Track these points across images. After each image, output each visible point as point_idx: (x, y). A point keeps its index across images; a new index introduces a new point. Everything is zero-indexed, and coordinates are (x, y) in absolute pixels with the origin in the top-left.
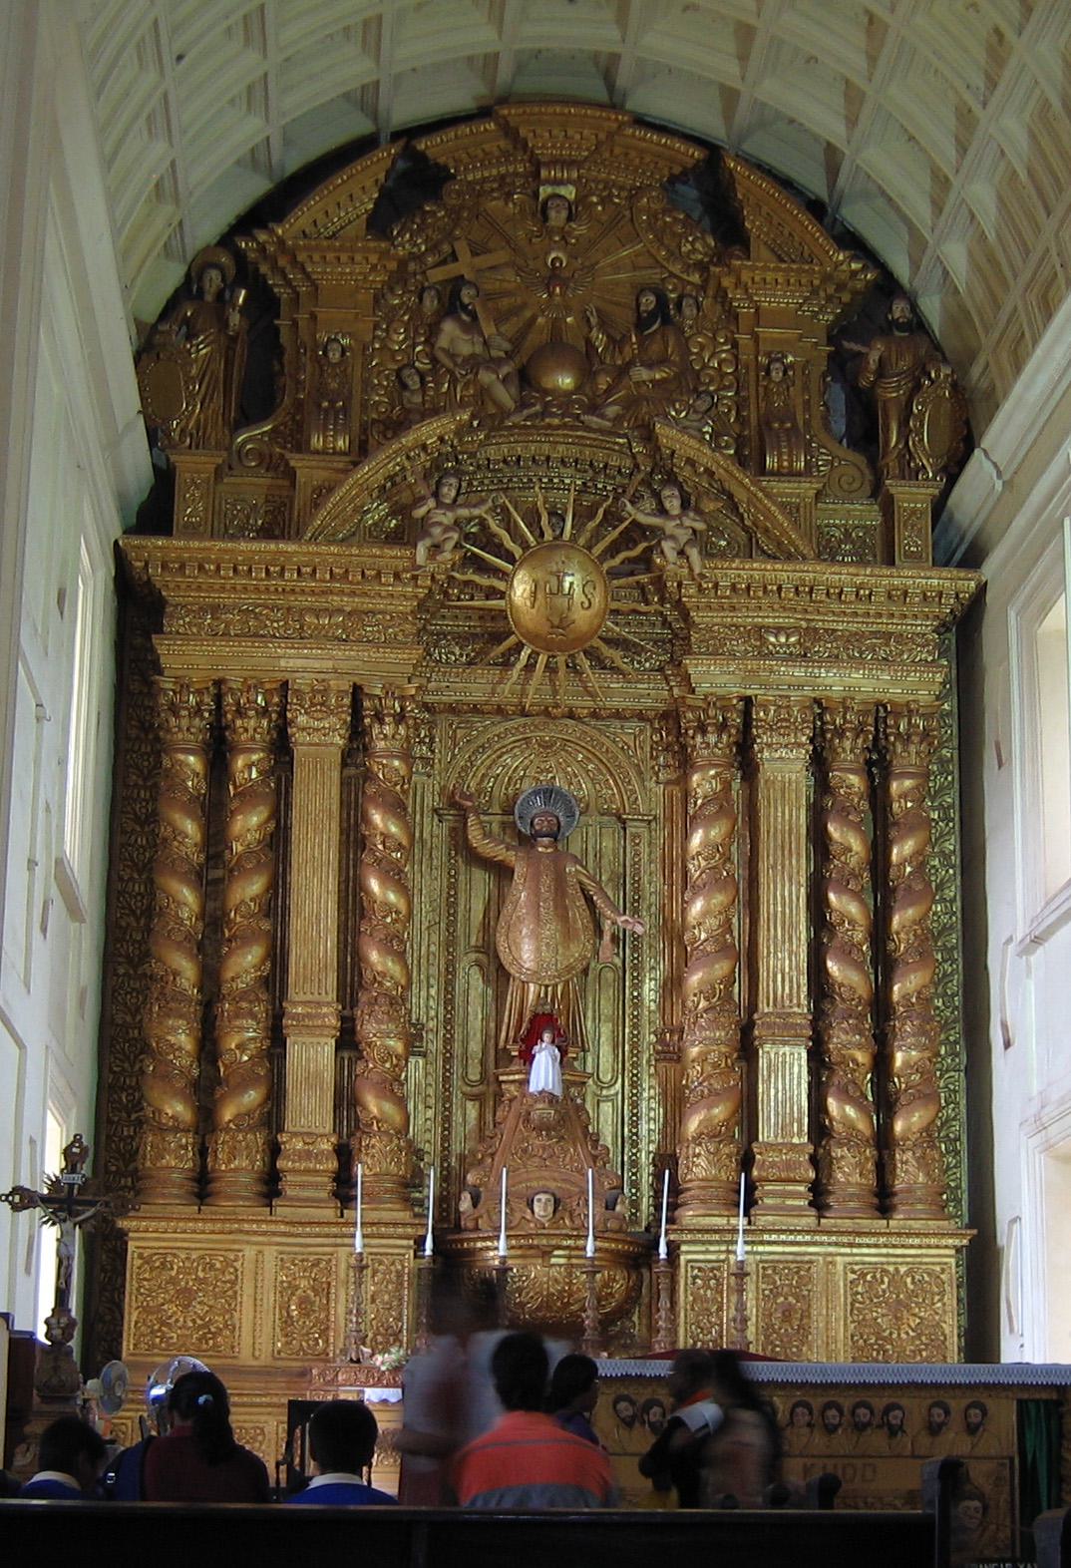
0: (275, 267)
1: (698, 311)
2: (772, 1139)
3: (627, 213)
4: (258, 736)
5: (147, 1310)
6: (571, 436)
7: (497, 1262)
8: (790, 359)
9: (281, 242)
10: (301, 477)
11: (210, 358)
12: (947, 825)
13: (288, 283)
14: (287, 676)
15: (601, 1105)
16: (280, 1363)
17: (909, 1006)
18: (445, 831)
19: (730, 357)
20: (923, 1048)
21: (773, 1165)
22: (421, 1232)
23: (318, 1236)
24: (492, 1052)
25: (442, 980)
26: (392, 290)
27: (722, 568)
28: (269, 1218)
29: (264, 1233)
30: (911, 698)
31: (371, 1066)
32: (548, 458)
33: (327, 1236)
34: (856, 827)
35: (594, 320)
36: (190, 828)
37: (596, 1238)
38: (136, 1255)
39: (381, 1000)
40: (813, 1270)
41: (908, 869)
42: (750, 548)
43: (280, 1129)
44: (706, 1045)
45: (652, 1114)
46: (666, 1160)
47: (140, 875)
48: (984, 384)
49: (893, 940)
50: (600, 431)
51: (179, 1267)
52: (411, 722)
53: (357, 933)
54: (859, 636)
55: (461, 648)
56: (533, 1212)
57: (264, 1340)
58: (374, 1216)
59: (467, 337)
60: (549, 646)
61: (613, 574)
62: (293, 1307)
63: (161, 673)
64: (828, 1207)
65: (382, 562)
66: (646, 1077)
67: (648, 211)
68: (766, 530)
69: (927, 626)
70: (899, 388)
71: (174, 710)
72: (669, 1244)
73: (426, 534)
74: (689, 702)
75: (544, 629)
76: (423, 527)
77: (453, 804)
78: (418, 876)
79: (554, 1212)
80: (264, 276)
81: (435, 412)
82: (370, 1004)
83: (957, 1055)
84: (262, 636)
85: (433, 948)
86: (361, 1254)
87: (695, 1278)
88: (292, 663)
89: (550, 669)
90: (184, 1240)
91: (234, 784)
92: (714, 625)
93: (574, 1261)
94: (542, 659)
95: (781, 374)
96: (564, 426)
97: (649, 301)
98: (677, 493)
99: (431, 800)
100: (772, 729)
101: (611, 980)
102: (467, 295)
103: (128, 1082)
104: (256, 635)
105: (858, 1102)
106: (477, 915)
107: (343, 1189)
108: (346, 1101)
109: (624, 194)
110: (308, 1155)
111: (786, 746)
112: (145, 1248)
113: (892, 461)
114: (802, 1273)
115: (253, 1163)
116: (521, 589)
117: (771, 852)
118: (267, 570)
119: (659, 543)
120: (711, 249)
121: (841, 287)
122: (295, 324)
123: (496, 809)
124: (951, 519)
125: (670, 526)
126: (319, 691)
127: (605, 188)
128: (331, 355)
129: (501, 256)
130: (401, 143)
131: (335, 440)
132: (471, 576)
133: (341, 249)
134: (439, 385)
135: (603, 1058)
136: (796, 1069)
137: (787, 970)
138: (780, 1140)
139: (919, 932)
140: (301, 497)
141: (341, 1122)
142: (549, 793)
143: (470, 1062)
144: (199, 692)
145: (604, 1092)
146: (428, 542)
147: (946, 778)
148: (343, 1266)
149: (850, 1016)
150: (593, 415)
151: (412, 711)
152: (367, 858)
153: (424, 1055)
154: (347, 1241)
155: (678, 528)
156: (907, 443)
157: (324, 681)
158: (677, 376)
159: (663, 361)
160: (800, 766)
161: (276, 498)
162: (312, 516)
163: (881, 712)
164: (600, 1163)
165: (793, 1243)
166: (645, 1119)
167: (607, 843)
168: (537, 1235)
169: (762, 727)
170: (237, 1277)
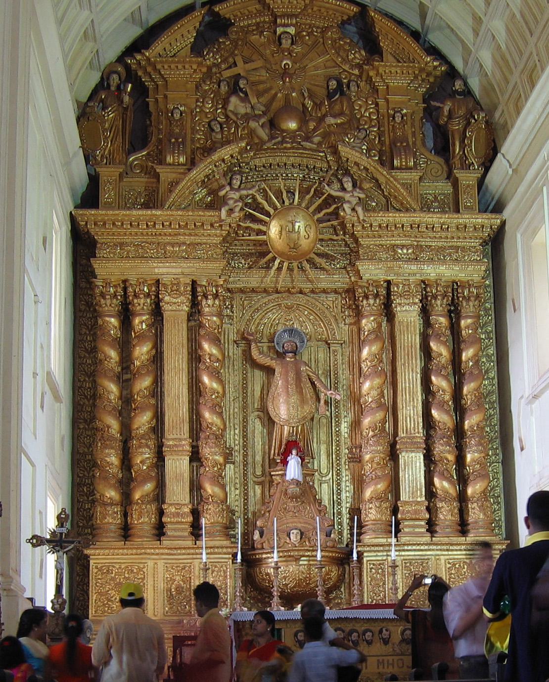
0: (146, 72)
1: (358, 88)
2: (407, 499)
3: (321, 40)
4: (145, 307)
5: (100, 594)
6: (297, 153)
7: (273, 564)
8: (405, 111)
9: (148, 59)
10: (162, 177)
11: (115, 118)
12: (489, 341)
13: (152, 80)
14: (159, 277)
15: (322, 485)
16: (167, 618)
17: (473, 431)
18: (240, 352)
19: (374, 111)
20: (481, 452)
21: (408, 512)
22: (235, 551)
23: (184, 554)
24: (267, 460)
25: (241, 426)
26: (204, 82)
27: (374, 217)
28: (159, 546)
29: (157, 554)
30: (470, 278)
31: (207, 469)
32: (285, 164)
33: (189, 554)
34: (444, 343)
35: (306, 95)
36: (113, 354)
37: (322, 551)
38: (94, 567)
39: (211, 437)
40: (430, 563)
41: (471, 364)
42: (387, 207)
43: (163, 502)
44: (373, 453)
45: (347, 489)
46: (355, 511)
47: (89, 379)
48: (502, 121)
49: (464, 399)
50: (310, 149)
51: (116, 572)
52: (221, 298)
53: (198, 403)
54: (443, 248)
55: (245, 260)
56: (290, 539)
57: (159, 605)
58: (211, 544)
59: (243, 105)
60: (289, 258)
61: (320, 221)
62: (173, 590)
63: (96, 278)
64: (436, 532)
65: (204, 219)
66: (344, 470)
67: (331, 39)
68: (395, 197)
69: (476, 242)
70: (459, 124)
71: (103, 295)
72: (358, 552)
73: (226, 204)
74: (359, 284)
75: (286, 250)
76: (224, 201)
77: (244, 338)
78: (227, 375)
80: (140, 76)
81: (229, 142)
82: (205, 439)
83: (498, 455)
84: (147, 257)
85: (236, 410)
86: (206, 562)
87: (371, 569)
88: (161, 270)
89: (290, 269)
90: (118, 559)
91: (134, 331)
92: (370, 245)
93: (311, 563)
94: (286, 264)
95: (400, 119)
96: (293, 148)
97: (333, 84)
98: (350, 180)
99: (233, 336)
100: (401, 296)
101: (325, 423)
102: (242, 84)
103: (87, 481)
104: (143, 257)
105: (449, 479)
106: (258, 393)
107: (196, 530)
108: (196, 487)
109: (319, 30)
110: (178, 514)
111: (408, 304)
112: (99, 563)
113: (457, 161)
114: (424, 565)
115: (150, 519)
116: (274, 230)
117: (403, 357)
118: (147, 224)
119: (342, 204)
120: (363, 56)
121: (428, 75)
122: (157, 100)
123: (265, 340)
124: (487, 188)
125: (347, 196)
126: (175, 284)
127: (310, 27)
128: (175, 115)
129: (259, 63)
130: (207, 7)
131: (179, 158)
132: (249, 224)
133: (178, 62)
134: (229, 129)
135: (322, 462)
136: (418, 464)
137: (412, 415)
138: (411, 500)
139: (477, 395)
140: (163, 187)
141: (194, 498)
142: (291, 331)
143: (256, 466)
144: (115, 286)
145: (324, 479)
146: (227, 208)
147: (488, 318)
148: (197, 568)
149: (444, 437)
150: (307, 141)
151: (222, 292)
152: (202, 366)
153: (234, 463)
154: (198, 556)
155: (351, 197)
156: (464, 151)
157: (177, 278)
158: (349, 122)
159: (341, 114)
160: (415, 314)
161: (150, 188)
162: (169, 197)
163: (455, 287)
164: (323, 514)
165: (419, 550)
166: (344, 491)
167: (321, 355)
168: (293, 550)
169: (396, 295)
170: (145, 576)
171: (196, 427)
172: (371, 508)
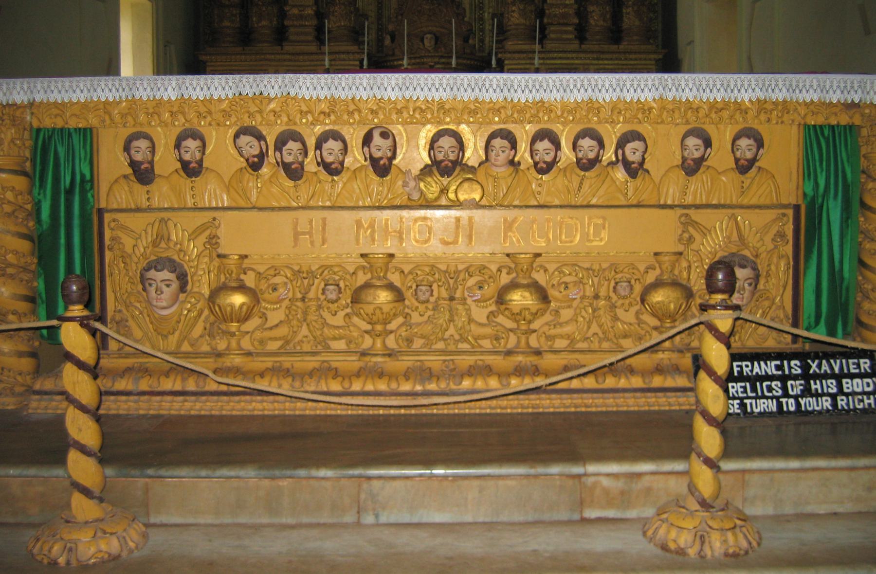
37: (457, 58)
79: (436, 43)
110: (301, 17)
172: (513, 11)
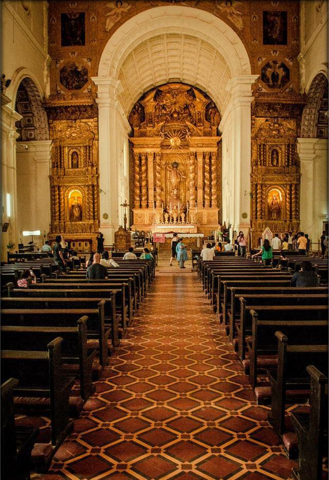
44: (192, 190)
108: (155, 196)
110: (151, 203)
129: (168, 101)
155: (189, 133)
159: (187, 113)
171: (155, 185)
